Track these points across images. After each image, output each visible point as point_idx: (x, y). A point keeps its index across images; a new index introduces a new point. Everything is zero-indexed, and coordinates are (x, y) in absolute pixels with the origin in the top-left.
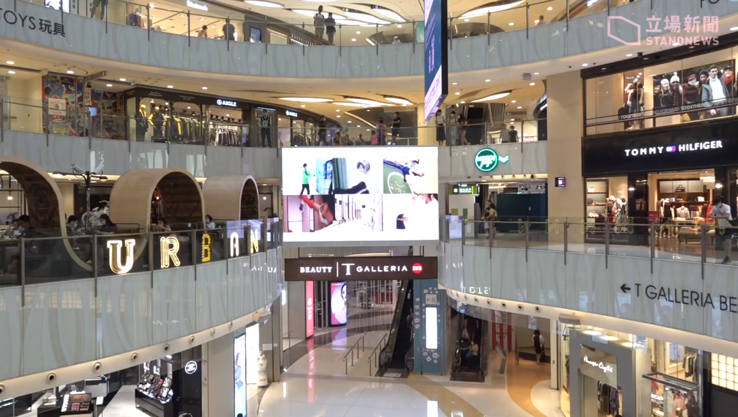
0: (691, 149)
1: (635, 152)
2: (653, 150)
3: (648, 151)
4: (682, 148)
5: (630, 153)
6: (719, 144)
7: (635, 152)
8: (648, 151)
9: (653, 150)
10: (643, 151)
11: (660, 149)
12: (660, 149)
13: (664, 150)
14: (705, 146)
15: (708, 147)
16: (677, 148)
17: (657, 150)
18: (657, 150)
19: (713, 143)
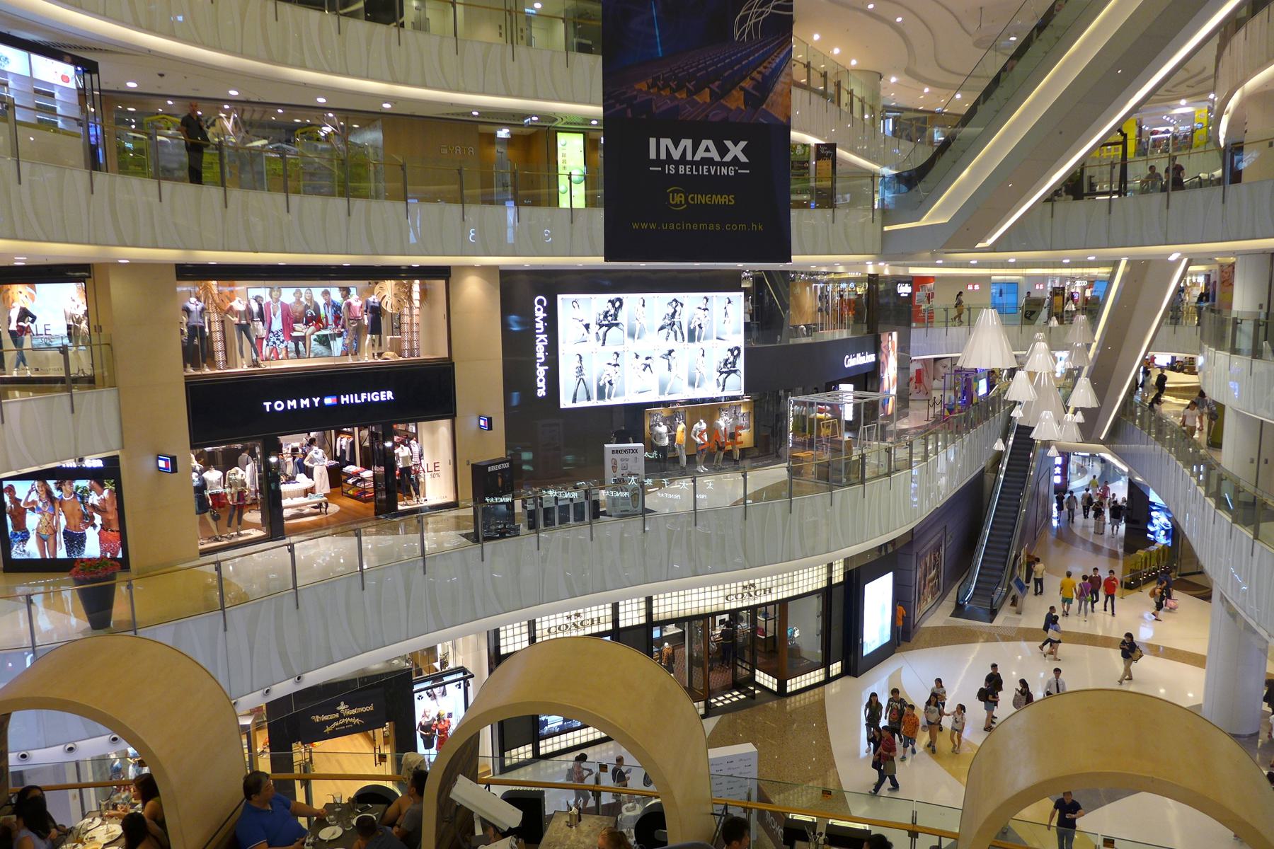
0: (357, 401)
1: (279, 406)
2: (305, 402)
3: (298, 404)
4: (344, 399)
5: (272, 407)
6: (390, 395)
7: (279, 406)
8: (298, 404)
9: (305, 402)
10: (292, 404)
11: (316, 401)
12: (316, 401)
13: (321, 402)
14: (374, 397)
15: (377, 399)
16: (339, 400)
17: (312, 403)
18: (312, 403)
19: (382, 393)
